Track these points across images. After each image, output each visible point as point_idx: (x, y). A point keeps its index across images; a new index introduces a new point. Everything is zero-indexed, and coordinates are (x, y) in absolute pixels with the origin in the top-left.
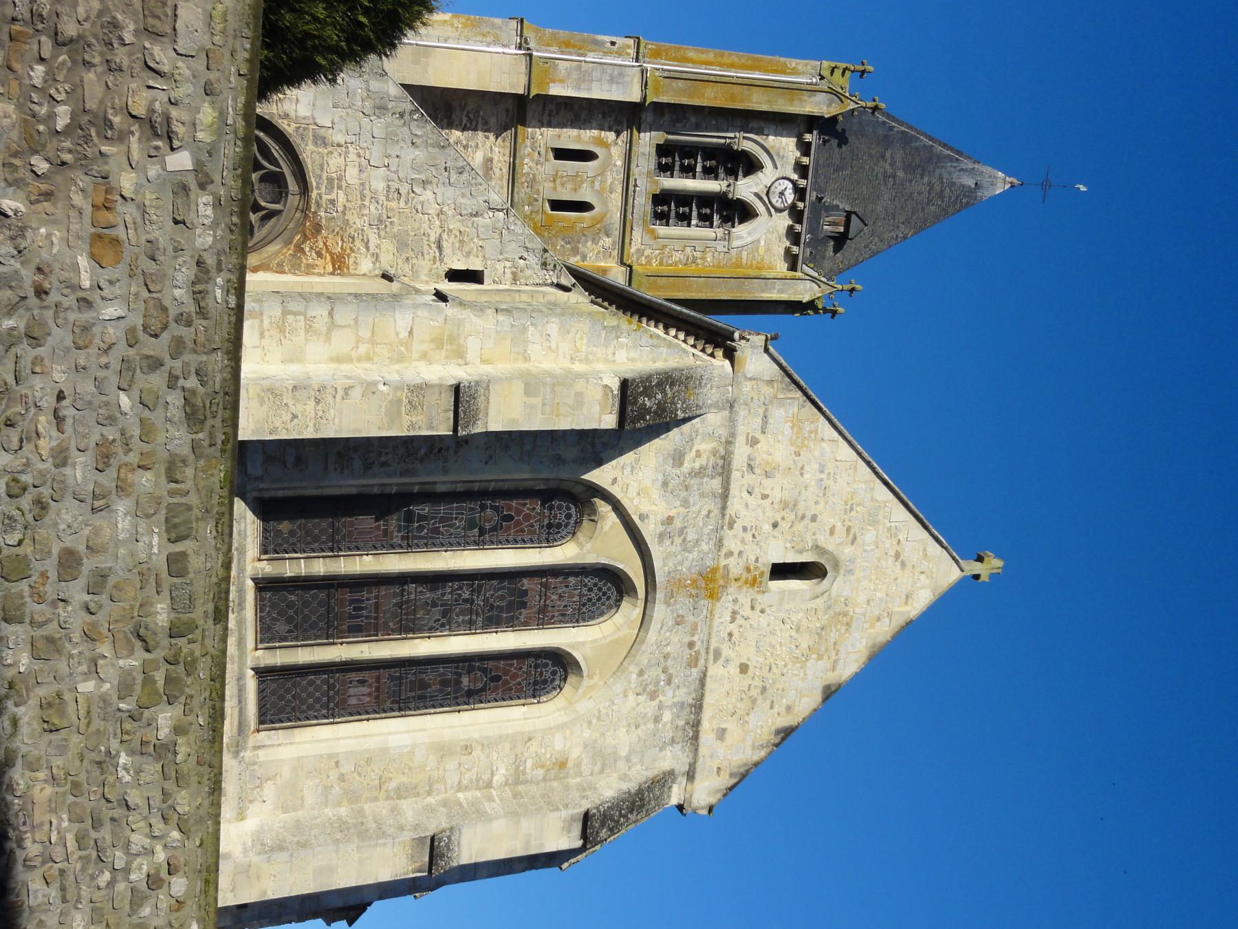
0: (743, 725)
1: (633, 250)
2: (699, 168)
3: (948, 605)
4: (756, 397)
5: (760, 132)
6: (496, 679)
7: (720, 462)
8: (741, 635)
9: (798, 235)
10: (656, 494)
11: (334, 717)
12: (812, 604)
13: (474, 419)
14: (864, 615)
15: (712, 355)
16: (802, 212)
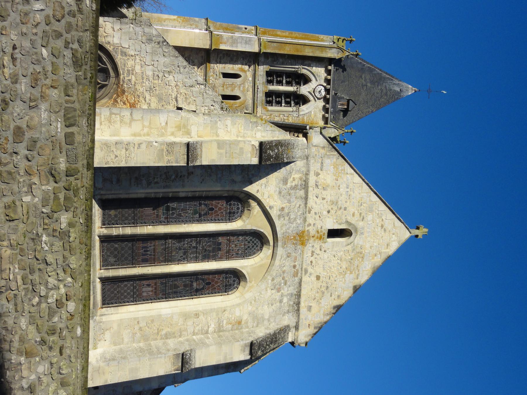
0: (319, 304)
2: (284, 82)
3: (406, 248)
4: (317, 154)
5: (309, 66)
6: (209, 284)
7: (304, 183)
8: (316, 262)
9: (328, 109)
10: (276, 197)
11: (136, 302)
12: (347, 248)
13: (195, 159)
14: (369, 253)
16: (329, 99)
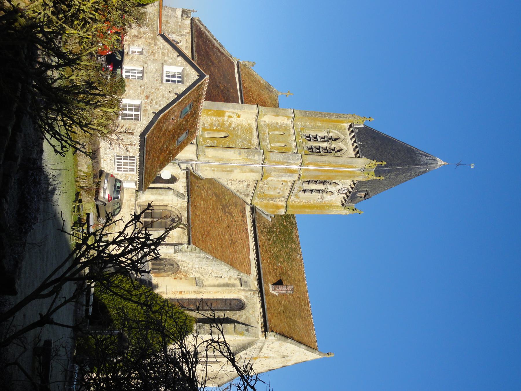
1: (291, 200)
15: (262, 332)
